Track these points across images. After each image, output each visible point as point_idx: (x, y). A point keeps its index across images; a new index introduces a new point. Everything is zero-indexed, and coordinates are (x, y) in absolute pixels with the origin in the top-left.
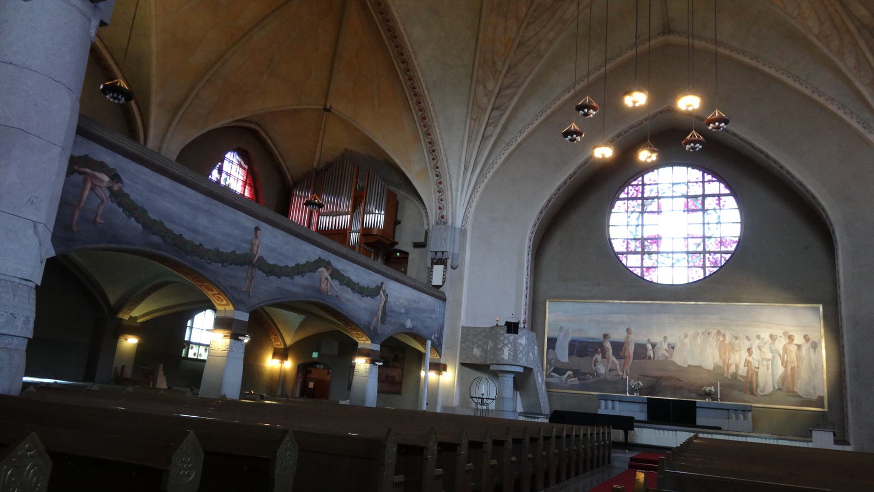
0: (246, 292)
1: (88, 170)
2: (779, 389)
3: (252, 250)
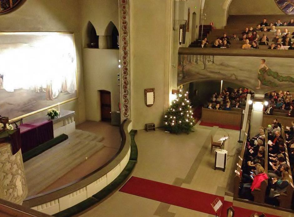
2: (61, 92)
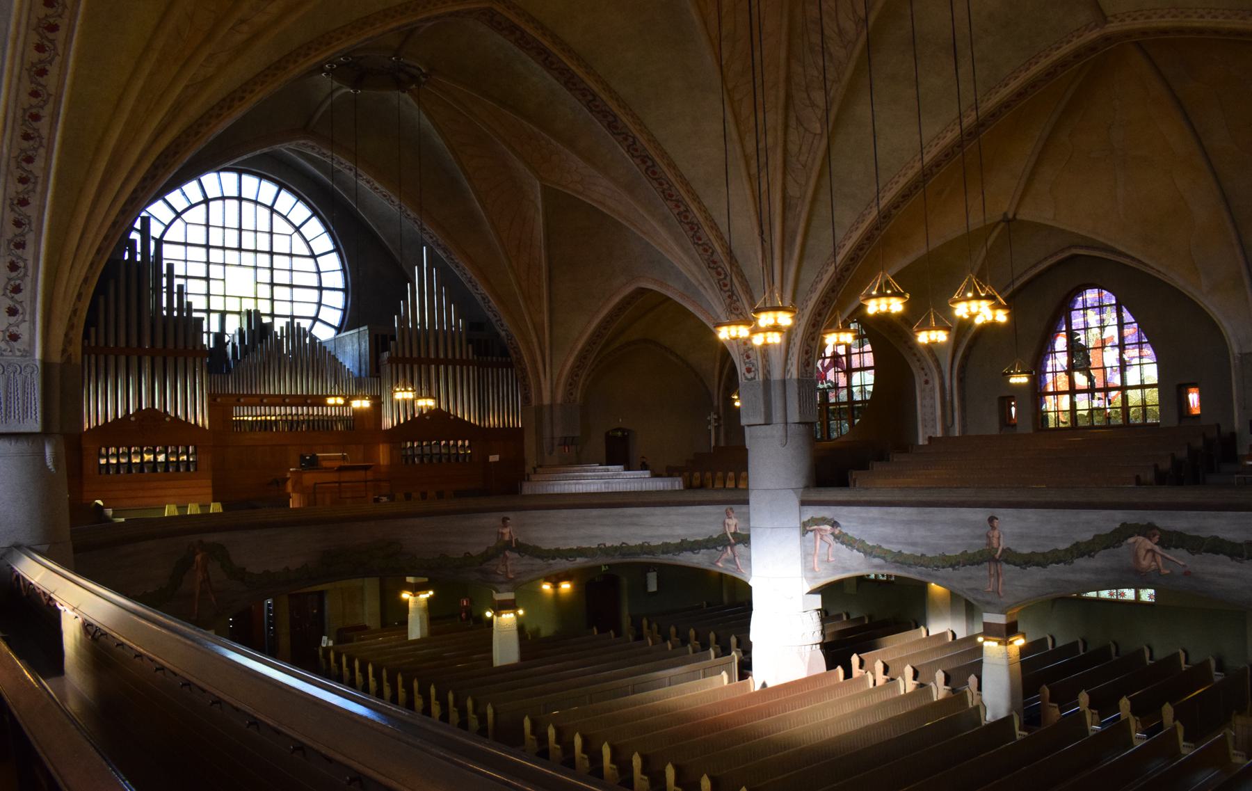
0: (993, 592)
1: (815, 527)
3: (990, 544)
